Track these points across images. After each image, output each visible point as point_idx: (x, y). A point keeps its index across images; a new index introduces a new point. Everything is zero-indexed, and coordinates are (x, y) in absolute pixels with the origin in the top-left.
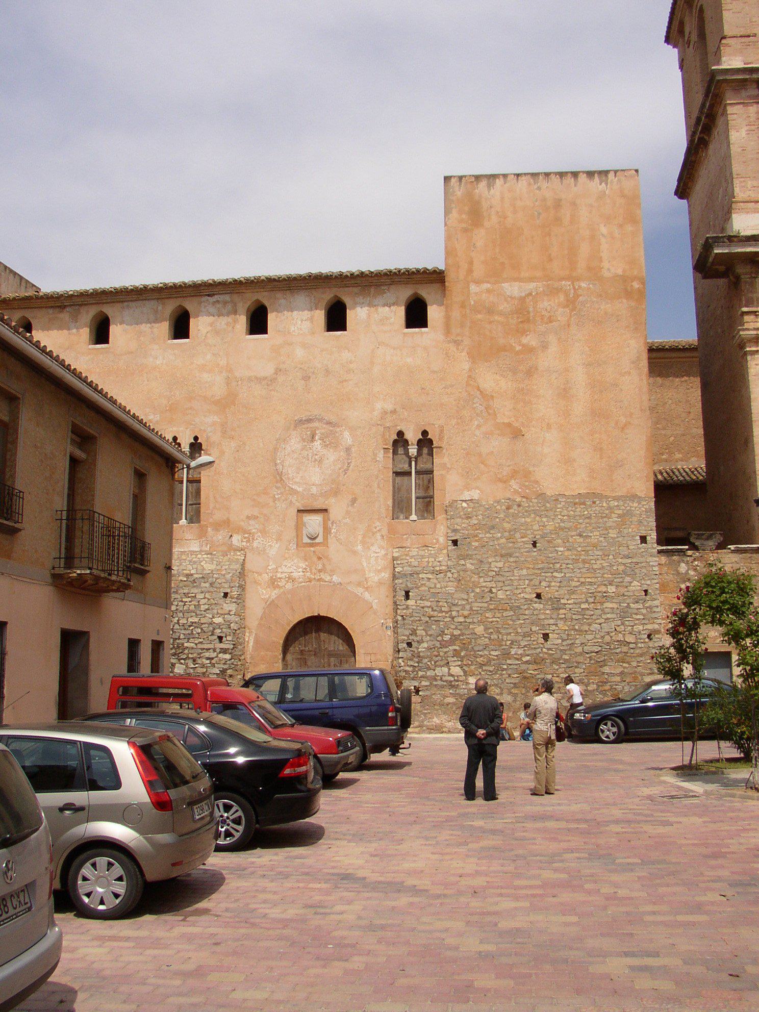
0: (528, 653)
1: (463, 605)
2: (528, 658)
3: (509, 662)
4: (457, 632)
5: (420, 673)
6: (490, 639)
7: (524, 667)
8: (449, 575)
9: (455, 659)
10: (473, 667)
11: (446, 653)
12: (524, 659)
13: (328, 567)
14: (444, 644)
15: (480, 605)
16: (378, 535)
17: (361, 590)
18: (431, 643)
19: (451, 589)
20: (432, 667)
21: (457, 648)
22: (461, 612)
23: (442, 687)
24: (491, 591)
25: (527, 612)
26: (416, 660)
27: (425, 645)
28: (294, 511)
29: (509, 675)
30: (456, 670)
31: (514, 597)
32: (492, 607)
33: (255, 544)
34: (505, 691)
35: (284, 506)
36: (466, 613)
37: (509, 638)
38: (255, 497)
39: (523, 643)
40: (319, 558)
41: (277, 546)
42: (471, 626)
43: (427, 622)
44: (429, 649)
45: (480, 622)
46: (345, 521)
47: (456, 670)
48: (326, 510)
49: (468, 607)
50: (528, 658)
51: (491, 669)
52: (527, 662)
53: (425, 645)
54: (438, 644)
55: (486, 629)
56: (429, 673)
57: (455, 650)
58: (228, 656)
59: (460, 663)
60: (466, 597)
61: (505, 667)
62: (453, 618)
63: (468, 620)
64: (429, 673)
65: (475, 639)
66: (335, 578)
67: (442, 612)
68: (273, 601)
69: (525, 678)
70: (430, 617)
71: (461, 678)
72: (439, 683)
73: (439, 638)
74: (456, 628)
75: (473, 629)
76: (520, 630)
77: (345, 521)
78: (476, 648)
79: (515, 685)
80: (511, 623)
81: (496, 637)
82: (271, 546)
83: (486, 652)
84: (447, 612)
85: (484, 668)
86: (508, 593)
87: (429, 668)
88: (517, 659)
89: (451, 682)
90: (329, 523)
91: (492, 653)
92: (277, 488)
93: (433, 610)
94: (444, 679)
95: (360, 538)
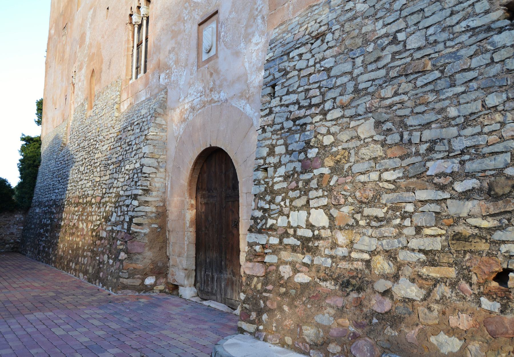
0: (469, 167)
1: (344, 85)
2: (470, 183)
3: (422, 195)
4: (328, 140)
5: (270, 222)
6: (383, 144)
7: (455, 208)
8: (329, 37)
9: (320, 193)
10: (346, 210)
11: (307, 182)
12: (459, 187)
13: (218, 83)
14: (307, 167)
15: (373, 75)
16: (259, 21)
17: (243, 102)
18: (290, 167)
19: (328, 63)
20: (286, 210)
21: (326, 171)
22: (338, 100)
23: (294, 249)
24: (395, 41)
25: (475, 62)
26: (268, 198)
27: (282, 171)
28: (196, 26)
29: (419, 230)
30: (320, 218)
31: (445, 36)
32: (393, 73)
33: (172, 79)
34: (408, 271)
35: (190, 26)
36: (345, 99)
37: (427, 135)
38: (173, 28)
39: (458, 145)
40: (211, 74)
41: (185, 74)
42: (353, 124)
43: (290, 129)
44: (286, 177)
45: (368, 111)
46: (231, 16)
47: (320, 218)
48: (217, 12)
49: (350, 87)
50: (470, 183)
51: (380, 213)
52: (466, 195)
53: (282, 171)
54: (298, 166)
55: (378, 124)
56: (282, 222)
57: (322, 175)
58: (135, 203)
59: (324, 201)
60: (347, 67)
61: (410, 208)
62: (324, 113)
63: (349, 112)
64: (282, 222)
65: (357, 149)
66: (223, 95)
67: (310, 106)
68: (181, 137)
69: (458, 237)
70: (294, 120)
71: (325, 233)
72: (291, 241)
73: (302, 156)
74: (329, 133)
75: (355, 128)
76: (453, 112)
77: (231, 16)
78: (356, 169)
79: (431, 258)
80: (431, 97)
81: (396, 138)
82: (181, 75)
83: (374, 176)
84: (317, 105)
85: (367, 211)
86: (431, 31)
87: (281, 213)
88: (442, 188)
89: (308, 240)
90: (219, 25)
91: (387, 176)
92: (186, 9)
93: (300, 108)
94: (300, 232)
95: (243, 31)
